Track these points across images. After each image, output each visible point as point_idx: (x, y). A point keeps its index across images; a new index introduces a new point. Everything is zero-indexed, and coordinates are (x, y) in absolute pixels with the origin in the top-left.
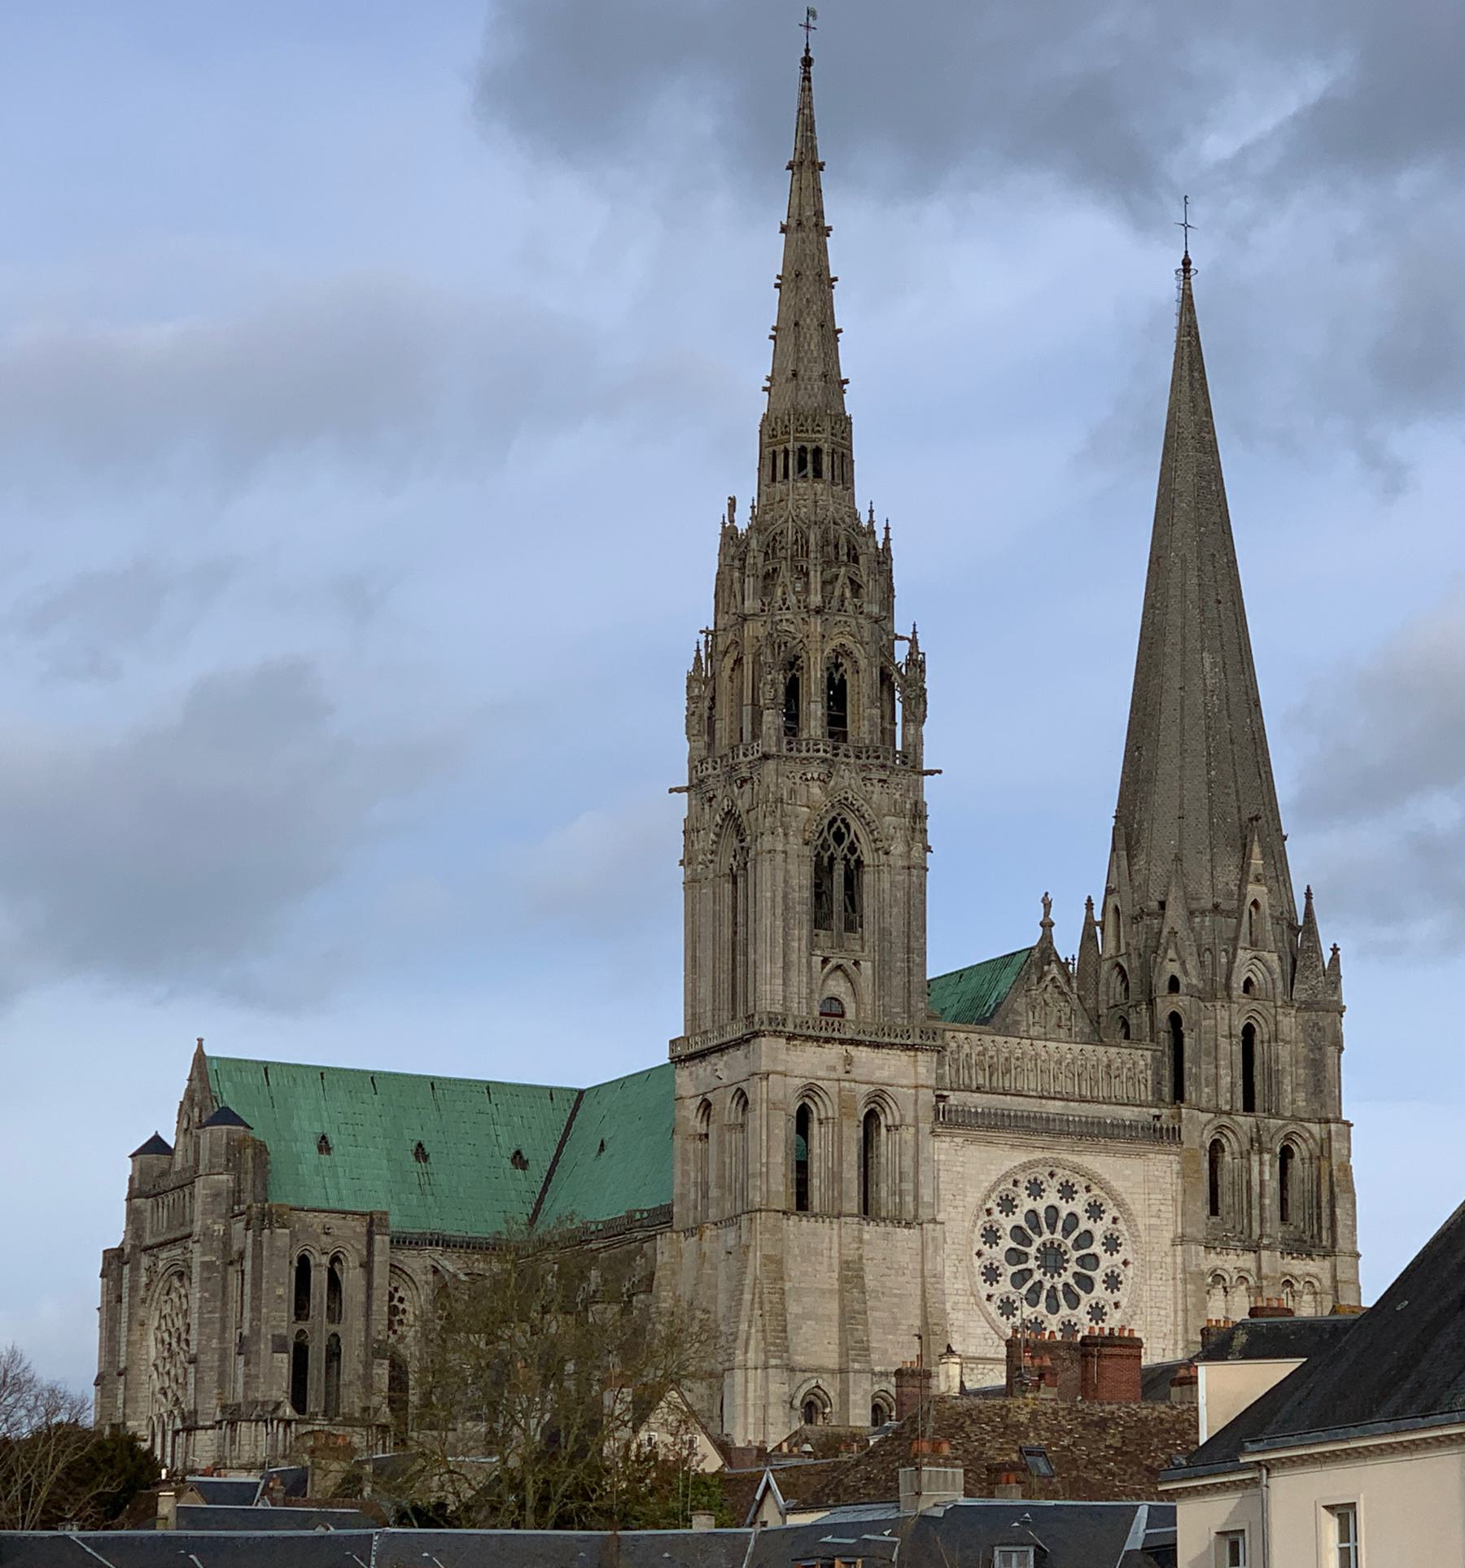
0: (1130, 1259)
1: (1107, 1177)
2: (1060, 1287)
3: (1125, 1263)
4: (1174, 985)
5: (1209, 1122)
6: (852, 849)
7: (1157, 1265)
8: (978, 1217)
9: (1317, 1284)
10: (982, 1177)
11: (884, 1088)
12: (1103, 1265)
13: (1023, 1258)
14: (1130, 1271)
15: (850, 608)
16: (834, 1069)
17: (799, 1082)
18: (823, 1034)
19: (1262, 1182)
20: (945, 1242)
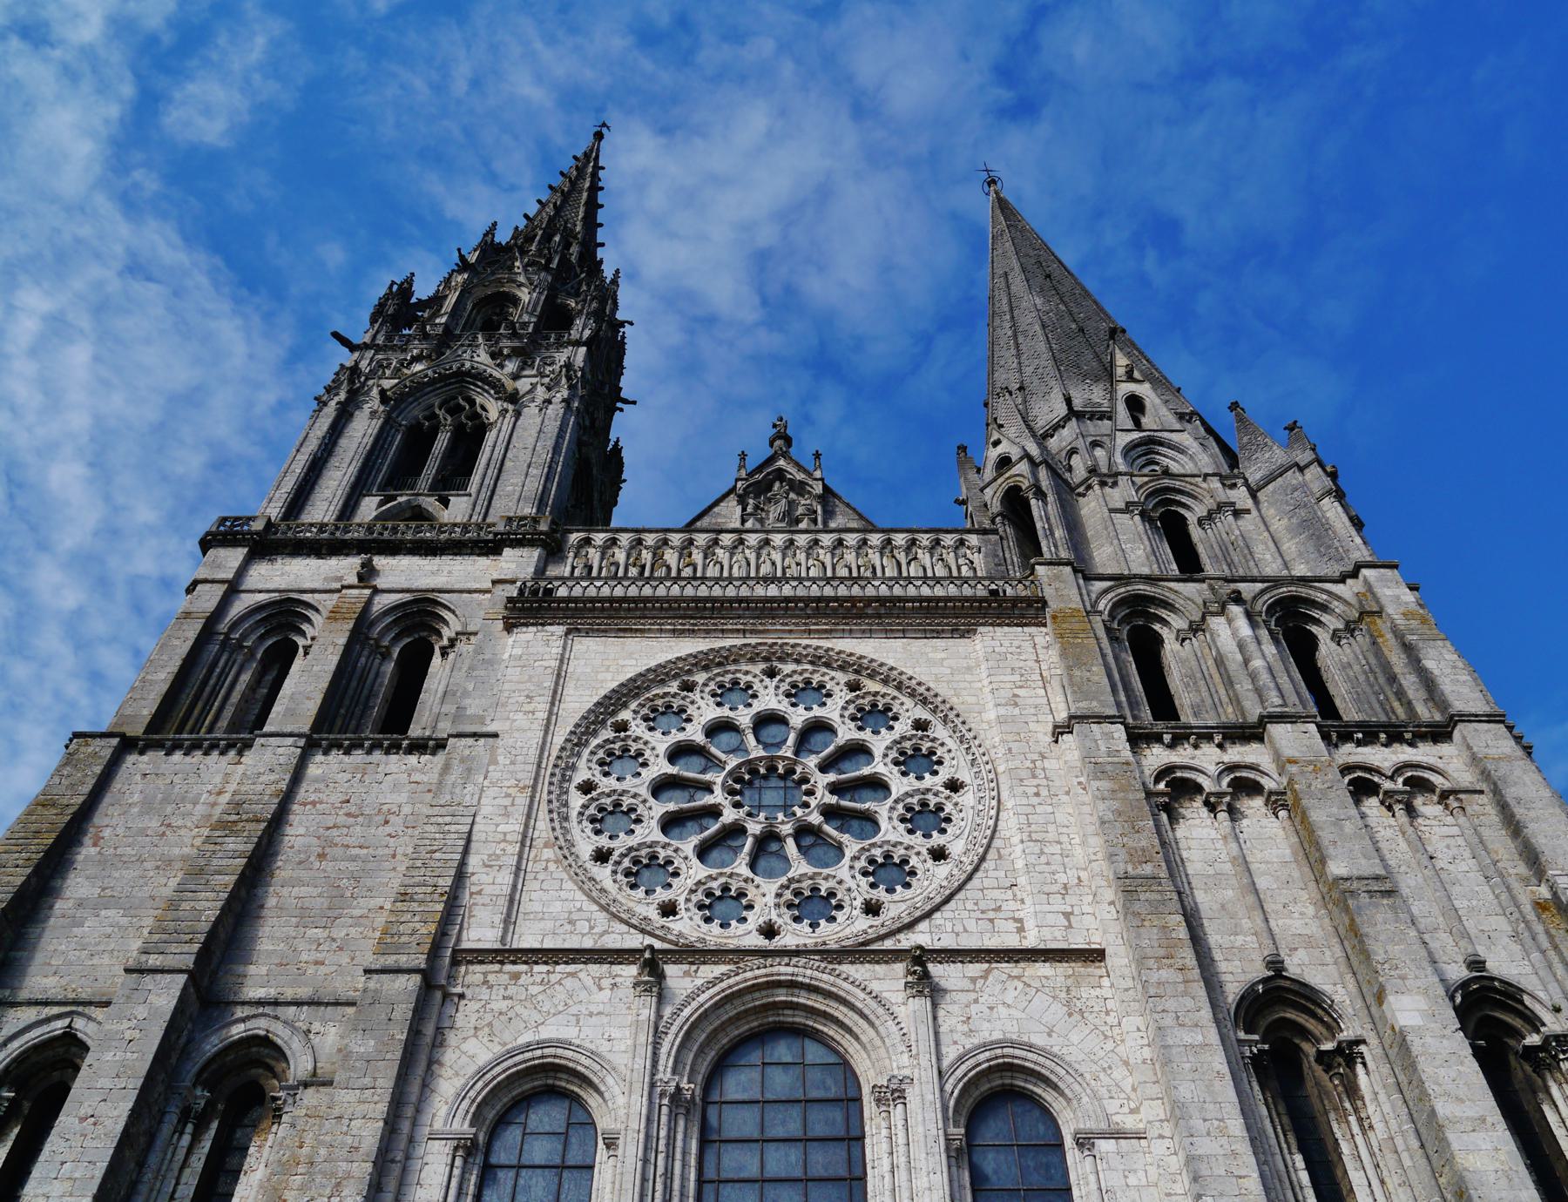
0: (964, 775)
1: (891, 663)
2: (787, 829)
3: (954, 786)
5: (1106, 591)
6: (475, 416)
7: (1024, 774)
9: (1436, 779)
10: (600, 677)
11: (430, 596)
13: (699, 794)
14: (967, 798)
16: (340, 579)
17: (261, 598)
19: (1241, 646)
20: (496, 763)
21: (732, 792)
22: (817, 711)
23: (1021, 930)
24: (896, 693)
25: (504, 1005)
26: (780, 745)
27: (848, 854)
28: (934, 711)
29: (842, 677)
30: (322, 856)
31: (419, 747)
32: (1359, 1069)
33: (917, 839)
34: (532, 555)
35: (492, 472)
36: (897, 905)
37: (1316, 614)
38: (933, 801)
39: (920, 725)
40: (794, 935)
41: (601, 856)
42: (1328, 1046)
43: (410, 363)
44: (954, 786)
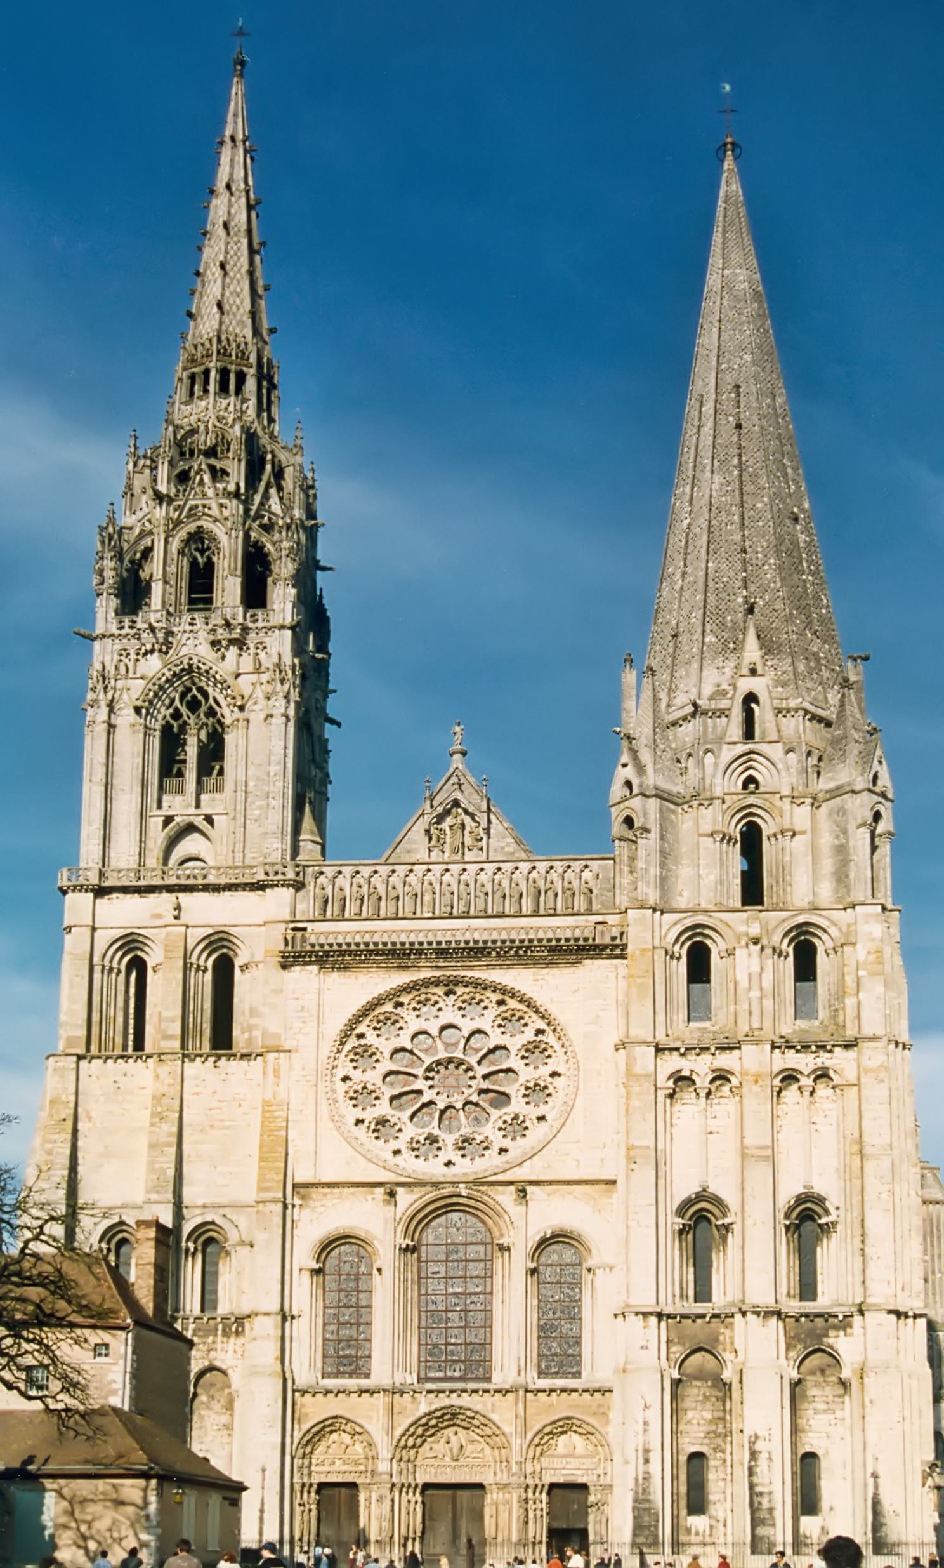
4: (628, 784)
8: (342, 1044)
12: (522, 1079)
15: (210, 493)
16: (160, 916)
18: (142, 883)
21: (427, 1078)
22: (478, 1024)
23: (578, 1165)
24: (525, 1009)
25: (321, 1209)
26: (456, 1045)
27: (493, 1119)
28: (549, 1024)
29: (495, 997)
30: (212, 1126)
31: (245, 1056)
32: (730, 1235)
33: (533, 1112)
34: (287, 893)
35: (241, 795)
36: (517, 1148)
37: (819, 932)
38: (542, 1084)
39: (540, 1032)
40: (465, 1168)
41: (359, 1122)
42: (719, 1223)
43: (145, 654)
44: (554, 1074)
